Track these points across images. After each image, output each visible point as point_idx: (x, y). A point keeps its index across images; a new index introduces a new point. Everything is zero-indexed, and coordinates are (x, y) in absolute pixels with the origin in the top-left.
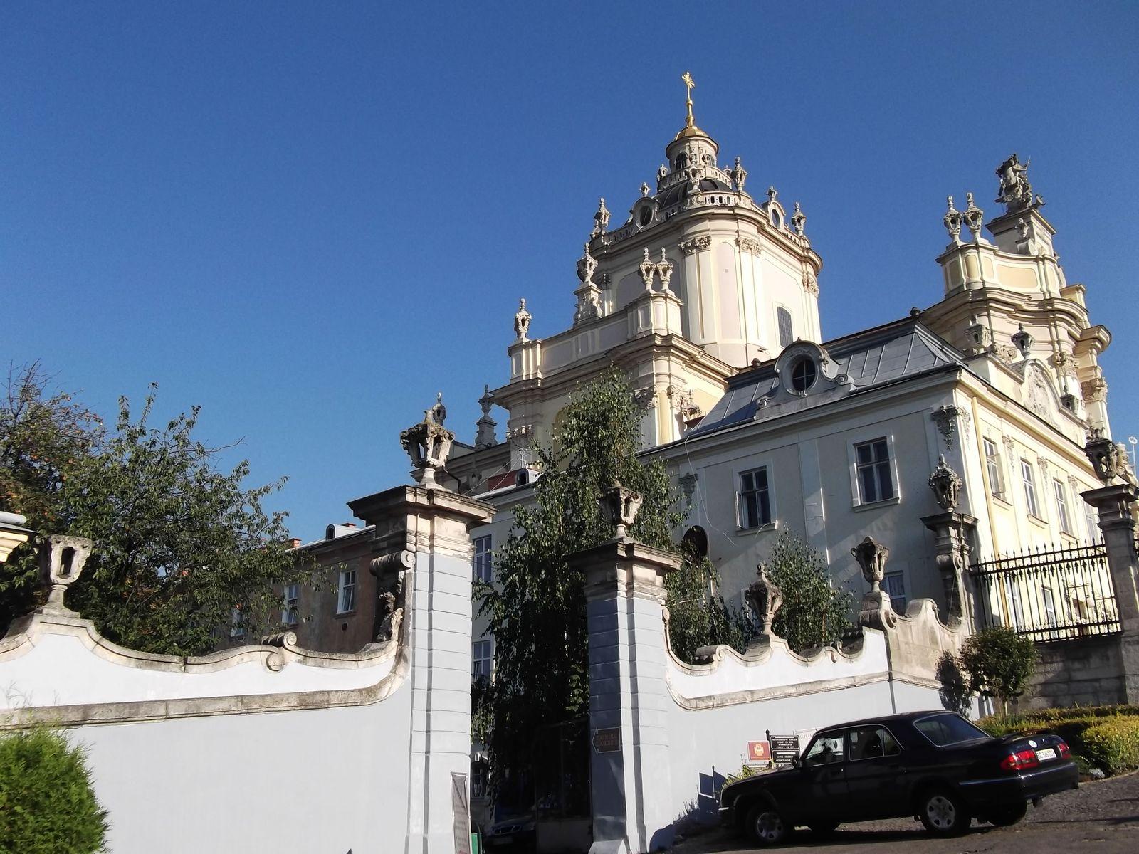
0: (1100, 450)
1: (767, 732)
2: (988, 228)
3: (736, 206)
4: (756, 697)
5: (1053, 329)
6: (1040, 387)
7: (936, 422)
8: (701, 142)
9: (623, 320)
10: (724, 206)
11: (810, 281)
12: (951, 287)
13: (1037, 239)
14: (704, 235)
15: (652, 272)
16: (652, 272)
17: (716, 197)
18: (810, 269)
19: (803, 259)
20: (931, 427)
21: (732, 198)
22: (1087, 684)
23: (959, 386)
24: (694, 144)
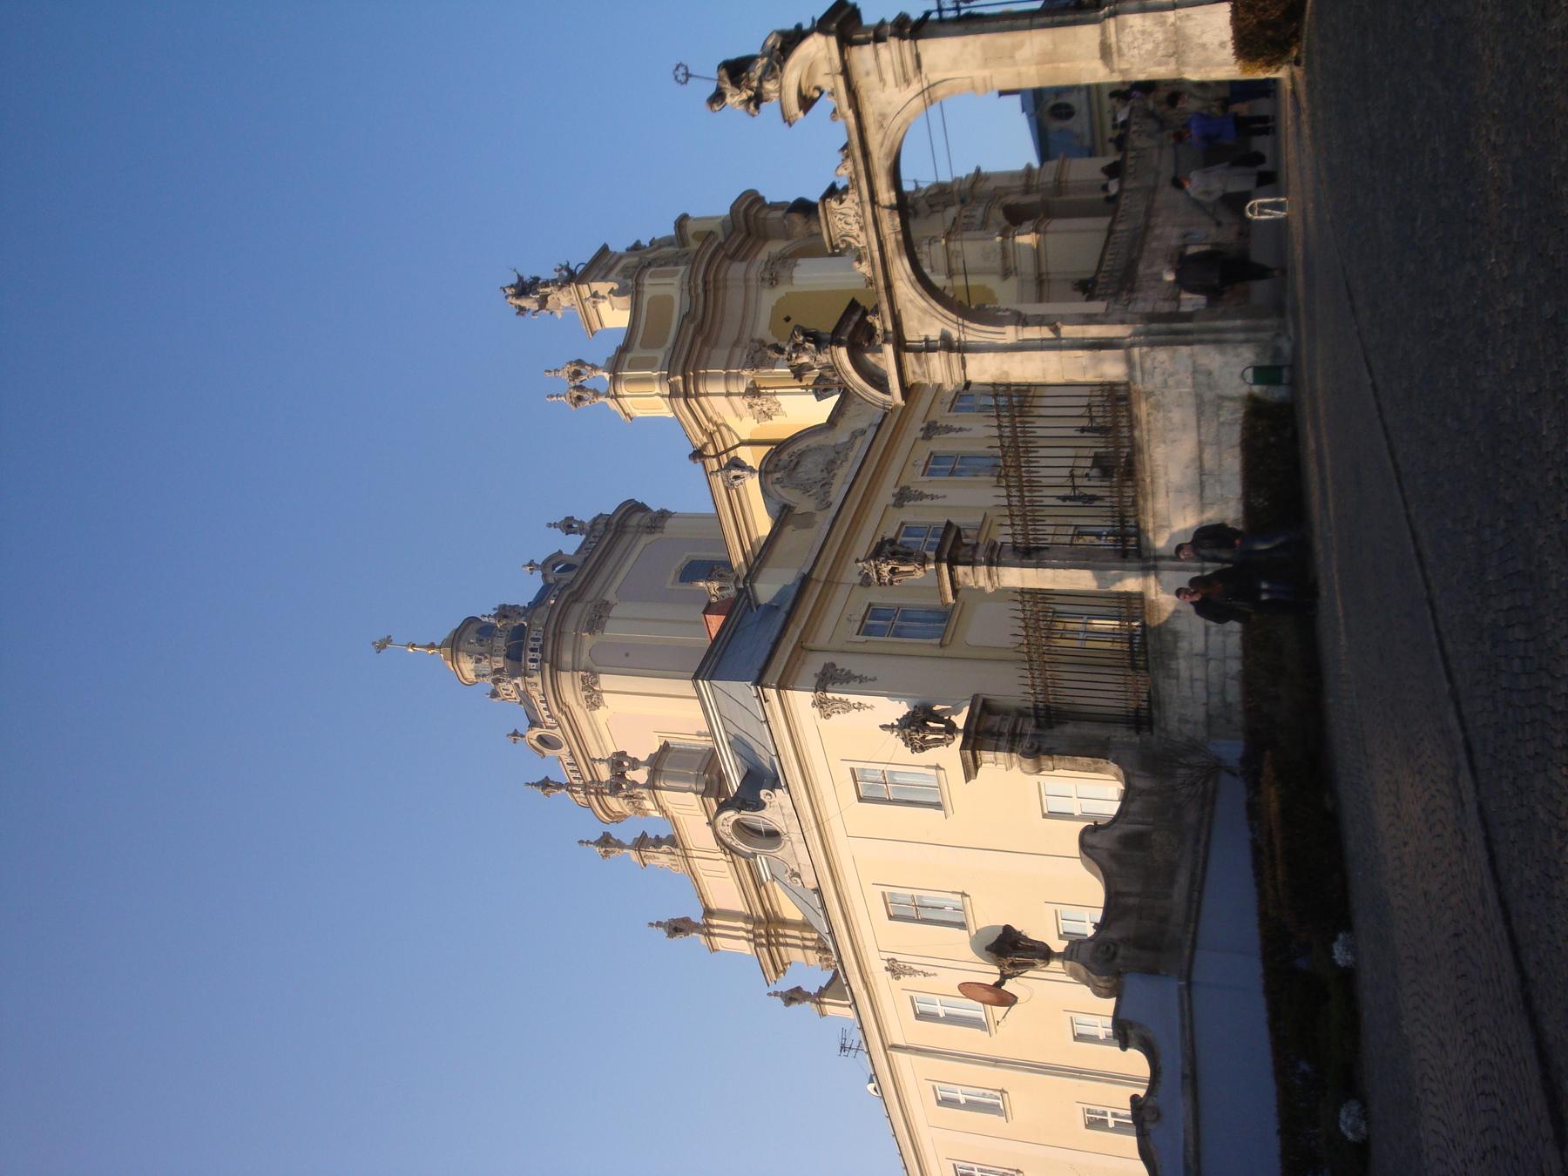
10: (542, 649)
18: (635, 520)
21: (533, 634)
22: (1212, 639)
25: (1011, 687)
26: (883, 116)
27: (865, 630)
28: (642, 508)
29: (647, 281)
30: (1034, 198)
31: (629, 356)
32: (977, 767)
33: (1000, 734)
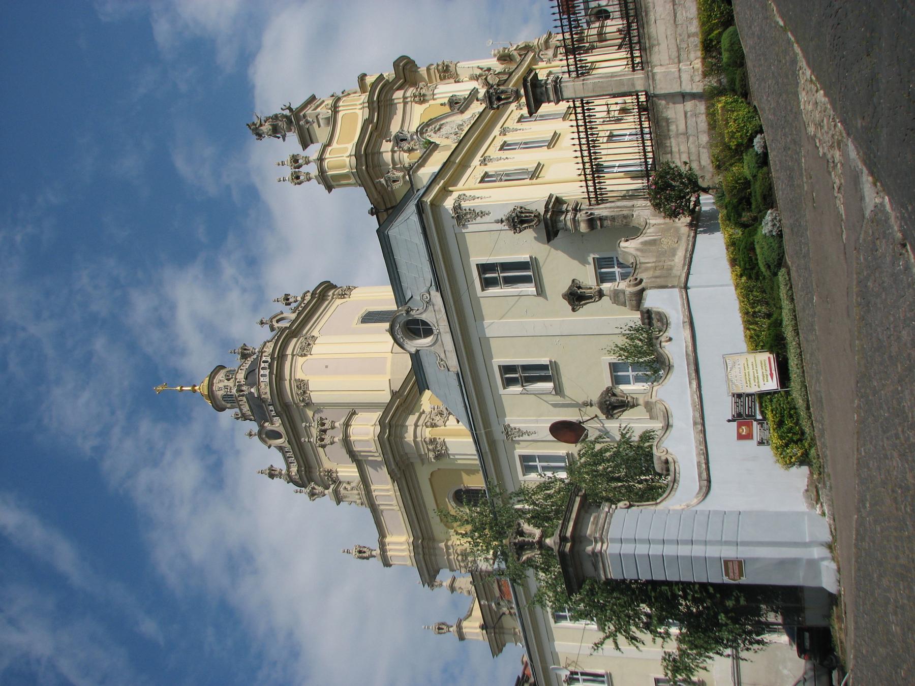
1: (729, 421)
4: (699, 420)
6: (439, 129)
12: (352, 181)
18: (331, 293)
21: (264, 359)
25: (573, 190)
28: (336, 287)
29: (341, 104)
31: (330, 148)
32: (556, 234)
33: (567, 211)
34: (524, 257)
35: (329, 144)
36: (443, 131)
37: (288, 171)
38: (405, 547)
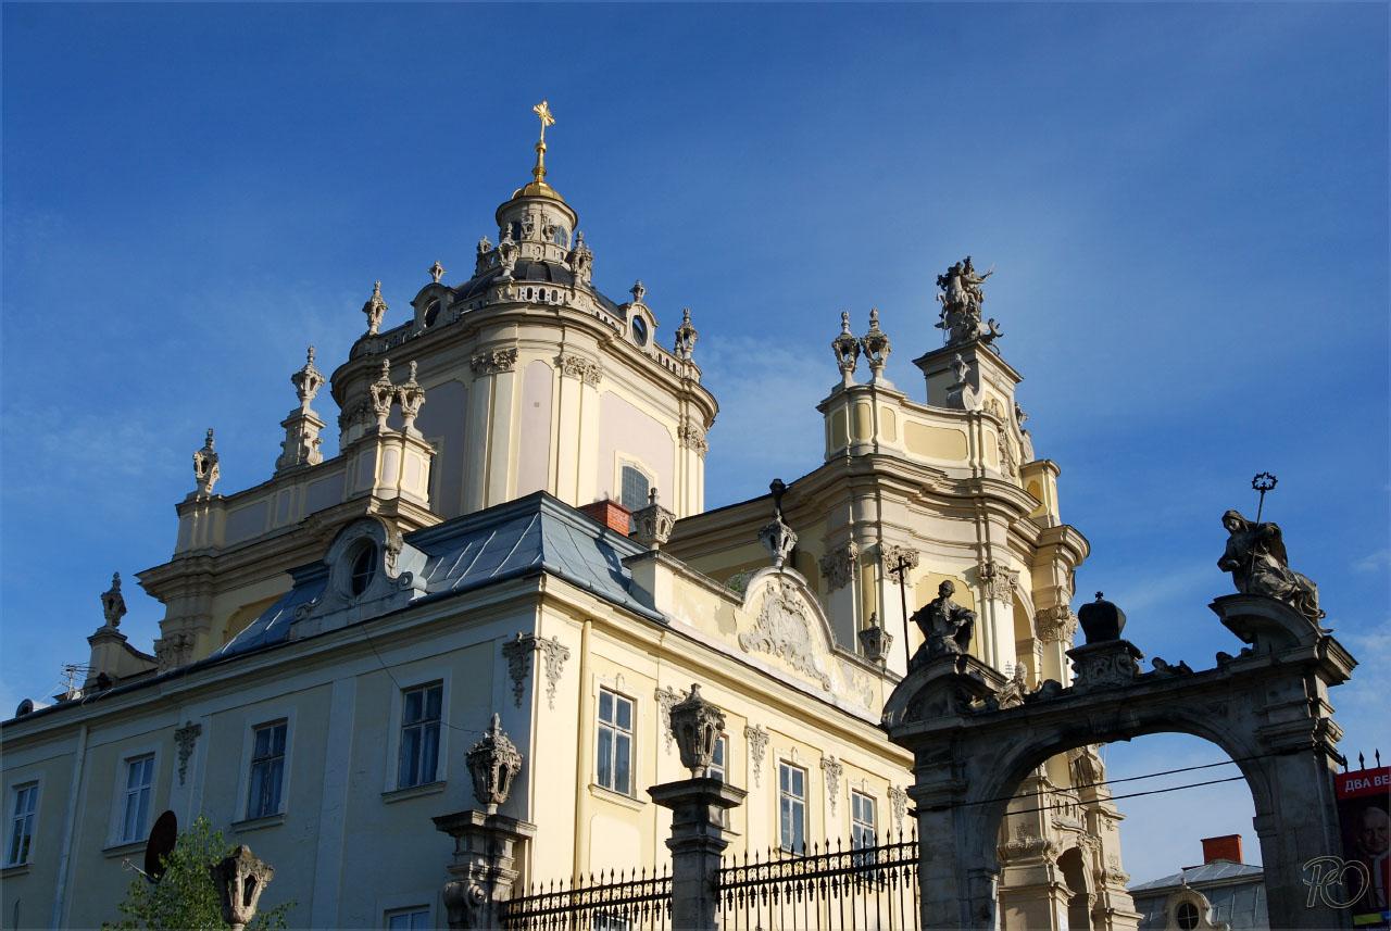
0: (688, 720)
2: (917, 364)
3: (565, 306)
5: (983, 525)
7: (508, 659)
8: (546, 207)
9: (339, 472)
10: (542, 304)
11: (690, 430)
12: (833, 451)
13: (984, 386)
14: (508, 347)
15: (389, 400)
16: (389, 400)
17: (536, 290)
18: (696, 414)
19: (683, 395)
20: (502, 667)
21: (561, 293)
23: (546, 599)
24: (535, 209)
26: (1224, 713)
27: (605, 701)
30: (1090, 887)
31: (894, 406)
34: (442, 773)
35: (904, 404)
36: (778, 616)
37: (856, 331)
38: (205, 543)
